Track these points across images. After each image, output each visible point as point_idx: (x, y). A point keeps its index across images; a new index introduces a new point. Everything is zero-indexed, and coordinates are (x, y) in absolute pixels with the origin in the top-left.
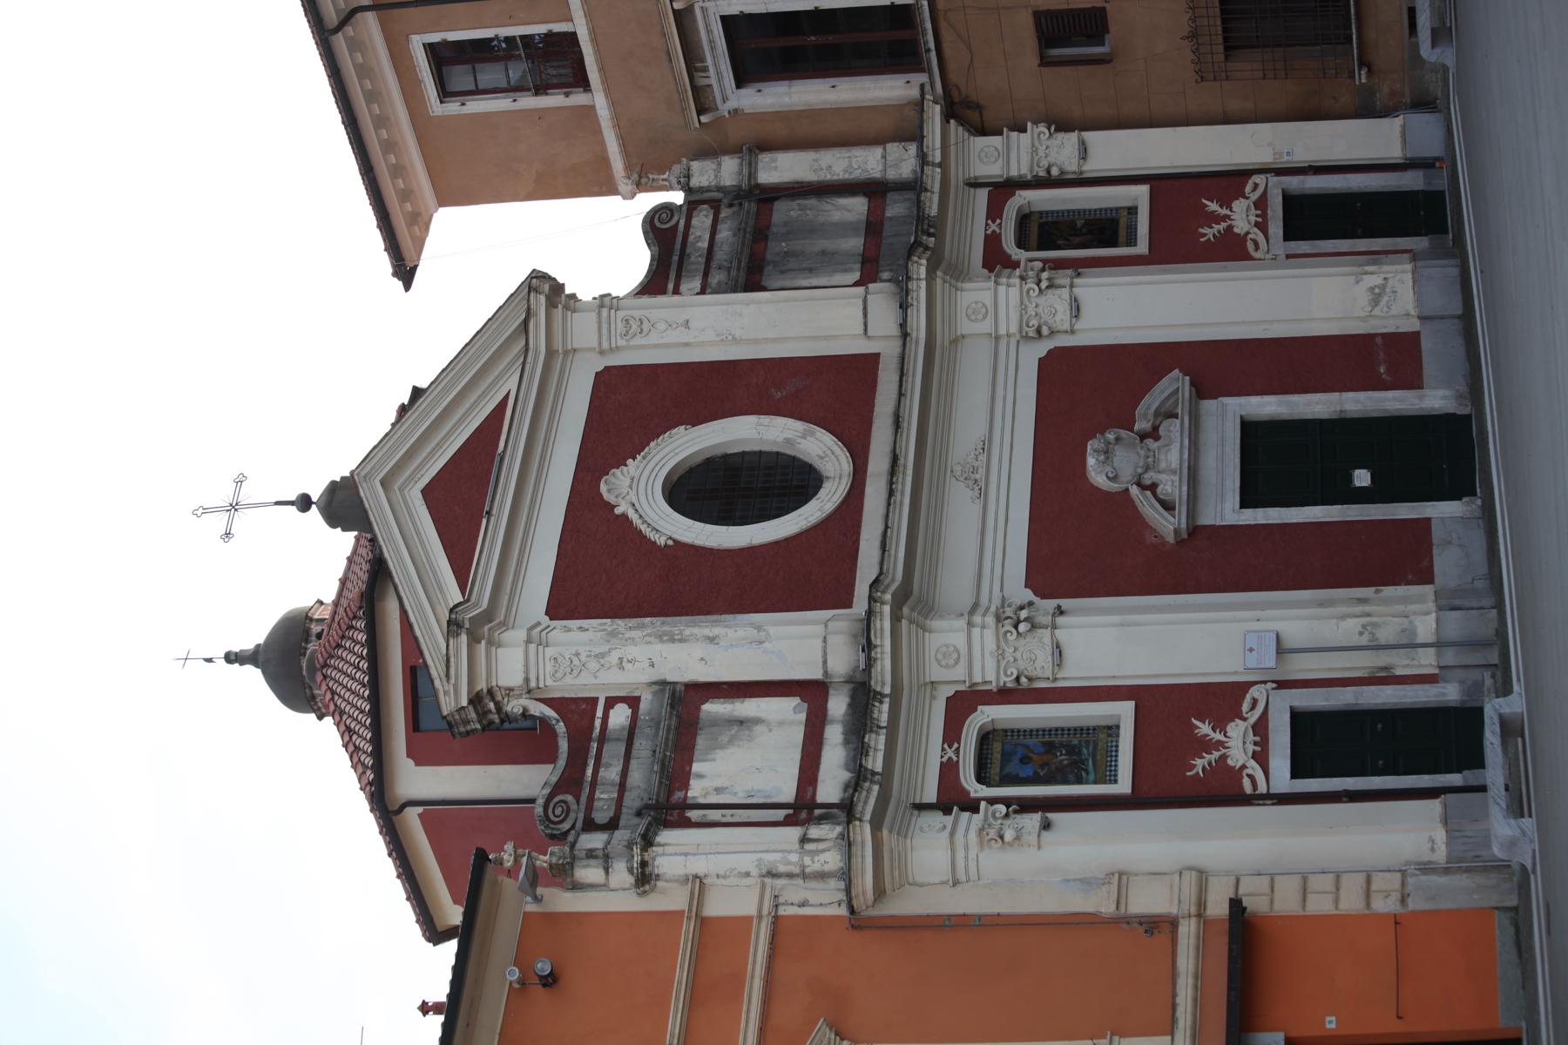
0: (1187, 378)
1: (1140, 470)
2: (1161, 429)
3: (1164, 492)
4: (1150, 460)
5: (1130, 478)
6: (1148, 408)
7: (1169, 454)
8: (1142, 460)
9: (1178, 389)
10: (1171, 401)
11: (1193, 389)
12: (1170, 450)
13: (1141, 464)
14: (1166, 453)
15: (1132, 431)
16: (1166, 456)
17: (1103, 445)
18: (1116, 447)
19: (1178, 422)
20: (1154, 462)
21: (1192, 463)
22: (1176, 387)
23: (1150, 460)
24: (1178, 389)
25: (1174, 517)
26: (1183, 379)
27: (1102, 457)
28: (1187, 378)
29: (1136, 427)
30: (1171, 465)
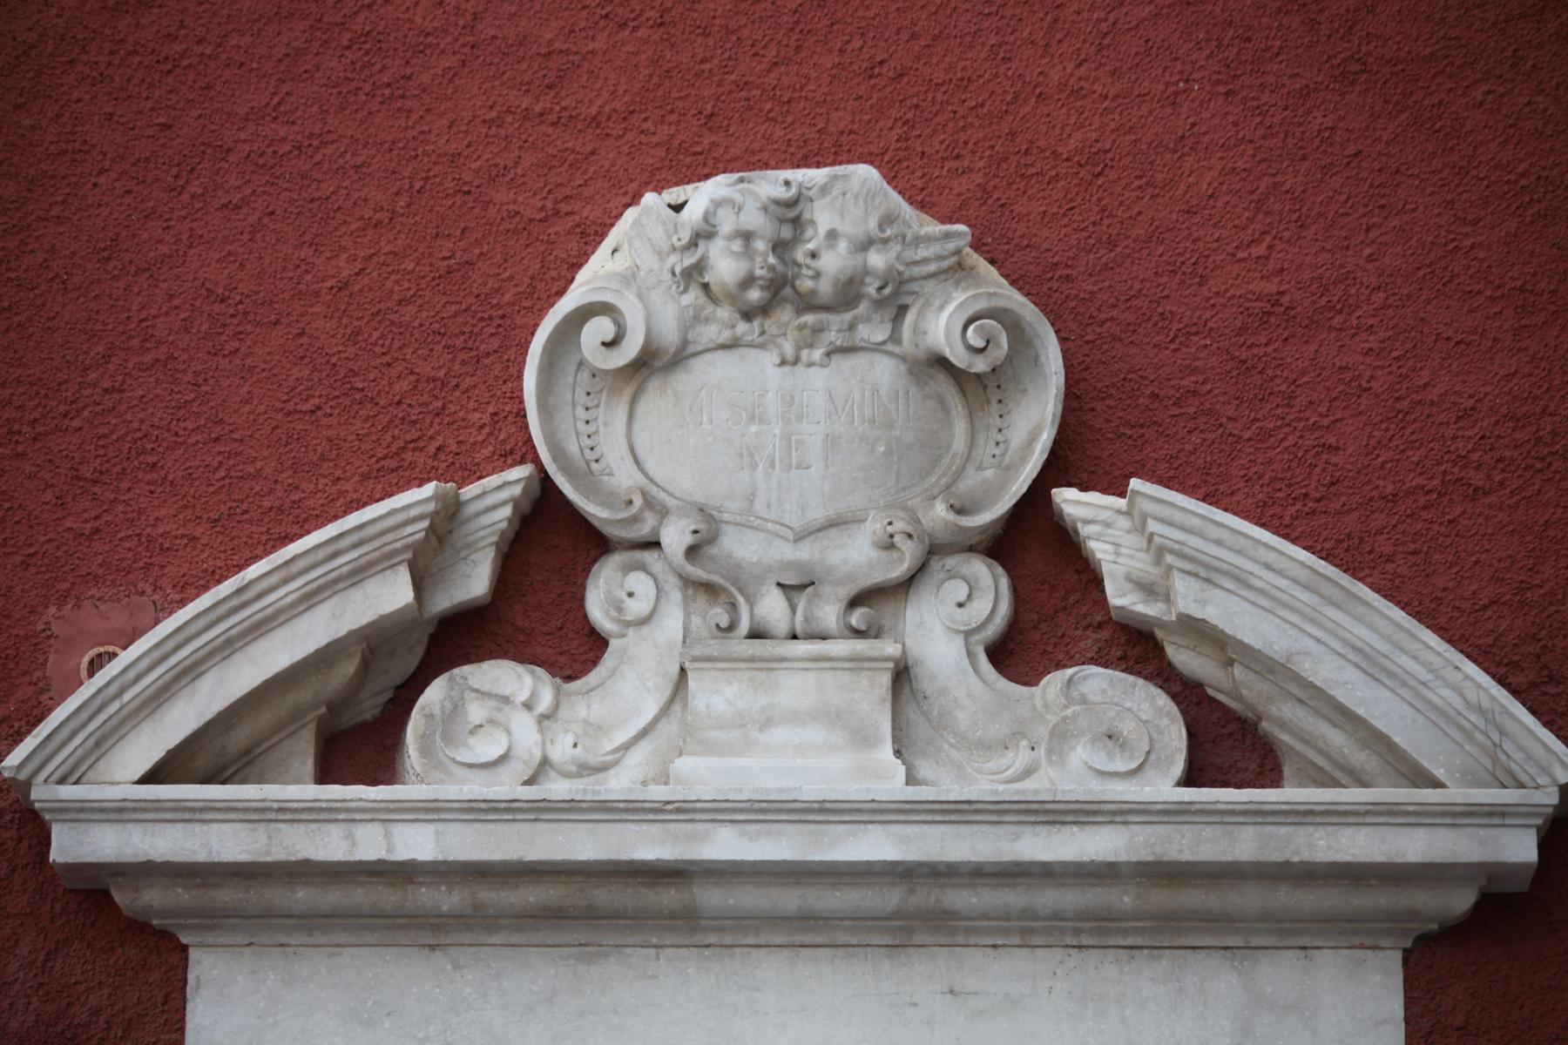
0: (1521, 848)
1: (675, 536)
2: (1098, 681)
3: (476, 712)
4: (773, 608)
5: (624, 477)
6: (1207, 573)
7: (816, 734)
8: (785, 552)
9: (1423, 778)
10: (1336, 738)
11: (1461, 901)
12: (863, 739)
13: (742, 547)
14: (825, 715)
15: (1058, 469)
16: (796, 718)
17: (834, 262)
18: (884, 372)
19: (1163, 787)
20: (756, 634)
21: (711, 897)
22: (1440, 773)
23: (773, 608)
24: (1437, 784)
25: (151, 777)
26: (1495, 815)
27: (725, 266)
28: (1521, 848)
29: (1069, 500)
30: (709, 749)
